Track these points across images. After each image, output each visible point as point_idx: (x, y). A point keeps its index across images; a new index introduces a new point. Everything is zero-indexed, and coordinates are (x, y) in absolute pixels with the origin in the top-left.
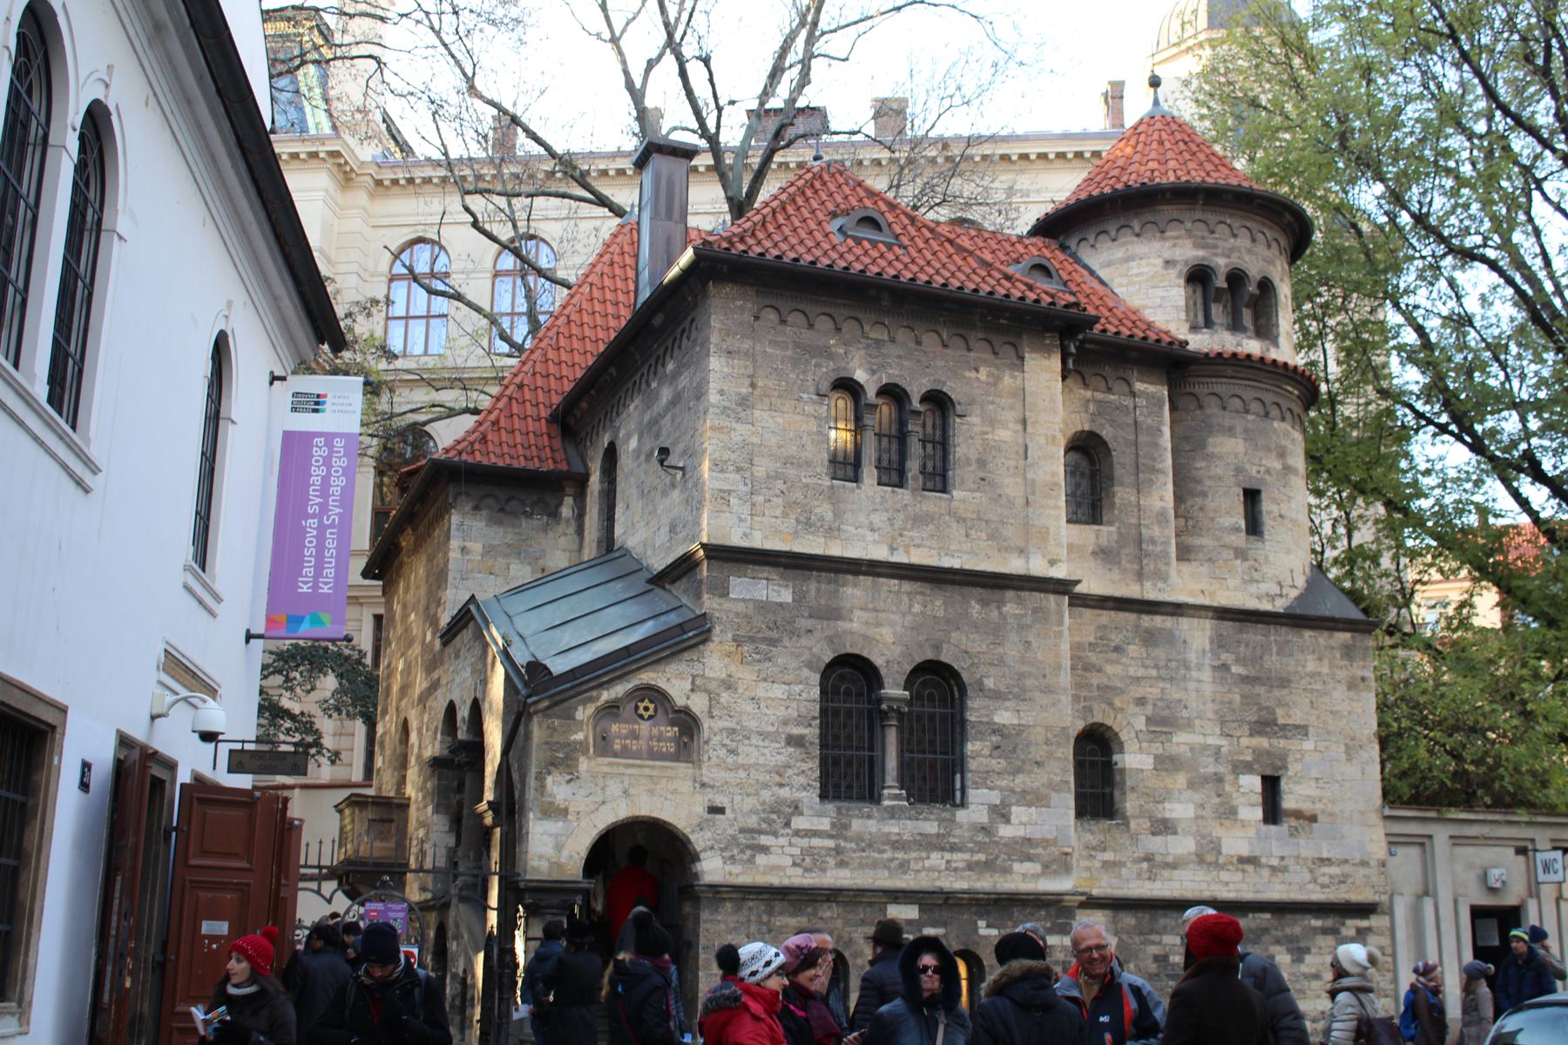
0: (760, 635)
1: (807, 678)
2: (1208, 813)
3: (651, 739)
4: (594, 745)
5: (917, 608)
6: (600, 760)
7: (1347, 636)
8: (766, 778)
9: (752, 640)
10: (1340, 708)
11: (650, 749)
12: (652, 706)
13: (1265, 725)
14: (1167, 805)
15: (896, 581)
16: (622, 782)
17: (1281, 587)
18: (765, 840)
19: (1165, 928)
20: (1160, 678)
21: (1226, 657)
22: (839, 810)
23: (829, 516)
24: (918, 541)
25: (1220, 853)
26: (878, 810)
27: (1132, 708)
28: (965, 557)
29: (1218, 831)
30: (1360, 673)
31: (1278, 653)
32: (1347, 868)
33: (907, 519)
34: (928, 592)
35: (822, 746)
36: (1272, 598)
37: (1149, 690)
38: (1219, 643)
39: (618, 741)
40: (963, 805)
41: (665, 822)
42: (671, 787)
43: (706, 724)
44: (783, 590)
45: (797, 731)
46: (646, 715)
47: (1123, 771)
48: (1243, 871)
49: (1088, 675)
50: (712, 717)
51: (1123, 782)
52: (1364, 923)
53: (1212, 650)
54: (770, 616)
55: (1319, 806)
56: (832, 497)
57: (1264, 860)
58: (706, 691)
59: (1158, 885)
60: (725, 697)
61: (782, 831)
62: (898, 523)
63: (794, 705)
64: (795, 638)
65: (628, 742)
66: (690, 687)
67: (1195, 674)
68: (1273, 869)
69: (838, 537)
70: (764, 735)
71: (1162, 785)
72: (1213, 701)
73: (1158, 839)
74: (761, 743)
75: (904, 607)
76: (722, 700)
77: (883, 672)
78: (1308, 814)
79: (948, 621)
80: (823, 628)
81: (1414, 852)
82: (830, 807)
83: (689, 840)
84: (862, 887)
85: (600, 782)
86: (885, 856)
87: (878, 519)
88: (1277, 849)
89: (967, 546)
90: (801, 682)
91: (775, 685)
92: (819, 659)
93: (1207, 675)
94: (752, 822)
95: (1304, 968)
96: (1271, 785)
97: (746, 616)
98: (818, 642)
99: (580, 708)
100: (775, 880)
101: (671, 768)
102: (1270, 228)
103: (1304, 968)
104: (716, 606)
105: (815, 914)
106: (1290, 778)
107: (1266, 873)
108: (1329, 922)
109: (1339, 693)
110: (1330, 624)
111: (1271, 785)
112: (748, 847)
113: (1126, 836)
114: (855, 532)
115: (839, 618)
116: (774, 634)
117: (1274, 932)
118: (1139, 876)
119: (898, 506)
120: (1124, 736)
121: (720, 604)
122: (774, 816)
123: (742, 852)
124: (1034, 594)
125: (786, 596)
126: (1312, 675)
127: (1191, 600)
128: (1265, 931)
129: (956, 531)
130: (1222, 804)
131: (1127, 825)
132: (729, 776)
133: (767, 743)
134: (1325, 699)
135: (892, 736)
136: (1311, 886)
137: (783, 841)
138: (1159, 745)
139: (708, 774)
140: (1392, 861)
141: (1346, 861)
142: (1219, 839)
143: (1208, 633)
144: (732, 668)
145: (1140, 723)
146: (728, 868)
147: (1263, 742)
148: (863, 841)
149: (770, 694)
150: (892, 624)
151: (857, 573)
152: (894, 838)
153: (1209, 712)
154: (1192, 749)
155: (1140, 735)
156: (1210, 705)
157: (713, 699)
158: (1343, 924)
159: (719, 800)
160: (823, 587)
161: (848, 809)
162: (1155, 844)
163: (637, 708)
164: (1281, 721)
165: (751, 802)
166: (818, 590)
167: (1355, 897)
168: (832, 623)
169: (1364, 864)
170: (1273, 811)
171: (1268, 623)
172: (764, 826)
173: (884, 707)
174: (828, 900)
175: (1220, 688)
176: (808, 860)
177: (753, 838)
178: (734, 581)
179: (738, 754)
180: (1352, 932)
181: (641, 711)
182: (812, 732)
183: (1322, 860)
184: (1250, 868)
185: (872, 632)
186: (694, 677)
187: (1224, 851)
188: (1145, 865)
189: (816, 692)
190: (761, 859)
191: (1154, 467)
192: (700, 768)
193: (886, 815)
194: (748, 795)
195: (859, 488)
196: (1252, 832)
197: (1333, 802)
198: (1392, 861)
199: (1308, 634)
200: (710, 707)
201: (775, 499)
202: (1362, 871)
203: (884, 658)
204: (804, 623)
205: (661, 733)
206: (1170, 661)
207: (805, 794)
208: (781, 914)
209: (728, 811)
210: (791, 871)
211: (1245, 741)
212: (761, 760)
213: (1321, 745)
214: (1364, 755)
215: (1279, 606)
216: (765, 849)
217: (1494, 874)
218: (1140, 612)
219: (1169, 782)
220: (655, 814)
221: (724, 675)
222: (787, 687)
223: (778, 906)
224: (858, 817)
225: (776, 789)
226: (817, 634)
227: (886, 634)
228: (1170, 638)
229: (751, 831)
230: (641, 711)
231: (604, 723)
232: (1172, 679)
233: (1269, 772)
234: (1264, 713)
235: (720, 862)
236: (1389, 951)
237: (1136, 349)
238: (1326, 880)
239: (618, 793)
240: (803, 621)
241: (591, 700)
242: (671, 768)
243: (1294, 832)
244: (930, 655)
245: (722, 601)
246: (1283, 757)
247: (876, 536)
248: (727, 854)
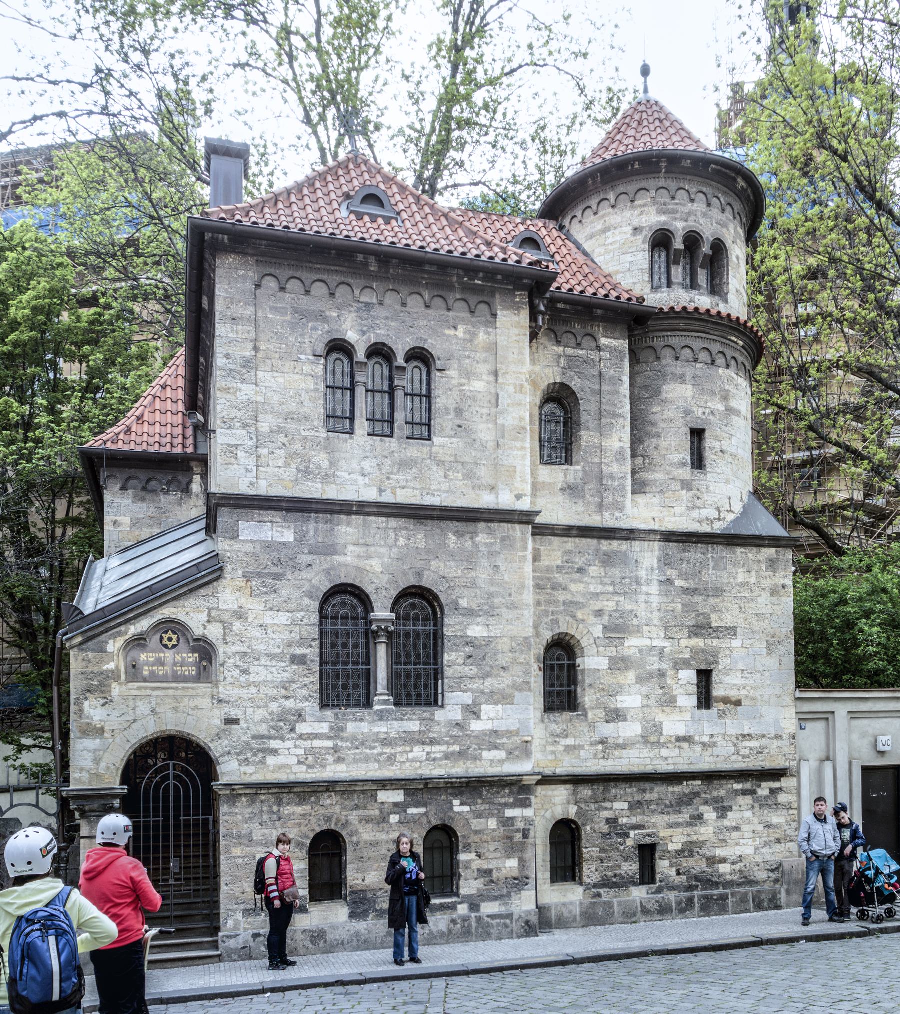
0: (266, 571)
1: (308, 606)
2: (652, 702)
5: (402, 541)
7: (773, 550)
8: (273, 692)
9: (260, 575)
10: (764, 611)
13: (701, 628)
14: (619, 698)
15: (384, 519)
17: (720, 512)
18: (274, 744)
19: (616, 796)
20: (615, 593)
21: (671, 573)
22: (336, 715)
23: (325, 464)
24: (403, 483)
25: (661, 734)
26: (369, 714)
27: (592, 619)
28: (444, 495)
29: (660, 717)
30: (782, 581)
31: (714, 569)
32: (764, 742)
33: (394, 464)
34: (411, 527)
35: (322, 663)
36: (711, 521)
37: (606, 603)
38: (666, 562)
40: (442, 706)
43: (221, 650)
44: (285, 531)
45: (299, 651)
47: (583, 671)
48: (680, 748)
49: (555, 593)
51: (584, 680)
52: (776, 785)
53: (659, 568)
54: (275, 554)
55: (743, 692)
56: (328, 447)
57: (697, 738)
58: (221, 621)
59: (610, 762)
60: (237, 626)
61: (288, 736)
62: (386, 469)
63: (297, 629)
67: (644, 588)
68: (704, 745)
69: (334, 482)
70: (271, 656)
71: (615, 681)
72: (659, 610)
73: (611, 726)
74: (269, 663)
75: (391, 541)
77: (373, 597)
78: (734, 699)
79: (428, 551)
80: (321, 563)
81: (820, 726)
82: (329, 713)
84: (356, 778)
85: (131, 703)
86: (375, 751)
87: (368, 465)
88: (708, 731)
89: (445, 486)
90: (302, 610)
92: (318, 589)
93: (654, 589)
94: (263, 729)
95: (726, 823)
96: (705, 677)
97: (254, 555)
98: (317, 574)
100: (283, 777)
102: (725, 193)
103: (726, 823)
104: (227, 548)
105: (317, 802)
106: (720, 671)
107: (698, 748)
108: (748, 786)
109: (764, 598)
110: (757, 541)
111: (705, 677)
112: (259, 750)
113: (584, 724)
114: (348, 477)
115: (335, 552)
116: (278, 570)
117: (703, 795)
118: (595, 755)
119: (386, 453)
120: (584, 643)
121: (231, 546)
122: (282, 724)
123: (255, 755)
124: (502, 524)
125: (289, 536)
126: (742, 585)
127: (643, 526)
128: (697, 794)
129: (437, 473)
130: (664, 695)
131: (586, 715)
132: (243, 693)
133: (274, 663)
134: (752, 605)
135: (382, 651)
136: (734, 758)
137: (289, 744)
138: (614, 649)
139: (224, 691)
140: (801, 735)
141: (764, 736)
142: (661, 723)
143: (657, 553)
144: (243, 601)
145: (598, 631)
146: (244, 769)
147: (699, 642)
148: (357, 740)
149: (276, 622)
150: (380, 556)
151: (350, 513)
152: (383, 736)
153: (656, 618)
154: (641, 651)
155: (598, 641)
156: (656, 614)
157: (227, 628)
158: (760, 786)
159: (234, 713)
160: (321, 526)
161: (344, 715)
162: (607, 730)
164: (714, 624)
165: (261, 713)
166: (317, 530)
167: (769, 764)
168: (329, 558)
169: (778, 737)
170: (705, 699)
171: (707, 543)
172: (273, 732)
173: (374, 627)
174: (328, 791)
175: (665, 599)
176: (311, 758)
177: (264, 743)
178: (242, 524)
179: (249, 674)
180: (766, 792)
182: (312, 652)
183: (744, 736)
184: (685, 745)
185: (363, 563)
186: (210, 610)
187: (665, 733)
188: (600, 747)
189: (315, 618)
190: (271, 760)
191: (614, 412)
193: (376, 718)
194: (259, 707)
195: (351, 438)
196: (688, 716)
197: (755, 688)
198: (801, 735)
199: (739, 550)
200: (225, 635)
201: (278, 451)
202: (776, 743)
203: (374, 586)
204: (304, 559)
206: (624, 578)
207: (307, 704)
208: (289, 804)
209: (242, 722)
210: (296, 769)
211: (684, 642)
212: (270, 678)
213: (747, 643)
214: (782, 649)
215: (718, 527)
216: (274, 752)
217: (882, 739)
218: (600, 538)
219: (621, 679)
221: (236, 607)
222: (290, 615)
223: (286, 798)
224: (352, 720)
226: (316, 568)
227: (376, 565)
228: (623, 559)
229: (262, 737)
232: (625, 593)
233: (703, 667)
234: (701, 618)
236: (795, 805)
237: (600, 306)
238: (747, 752)
240: (304, 557)
243: (722, 715)
244: (413, 581)
245: (233, 542)
246: (715, 655)
247: (367, 480)
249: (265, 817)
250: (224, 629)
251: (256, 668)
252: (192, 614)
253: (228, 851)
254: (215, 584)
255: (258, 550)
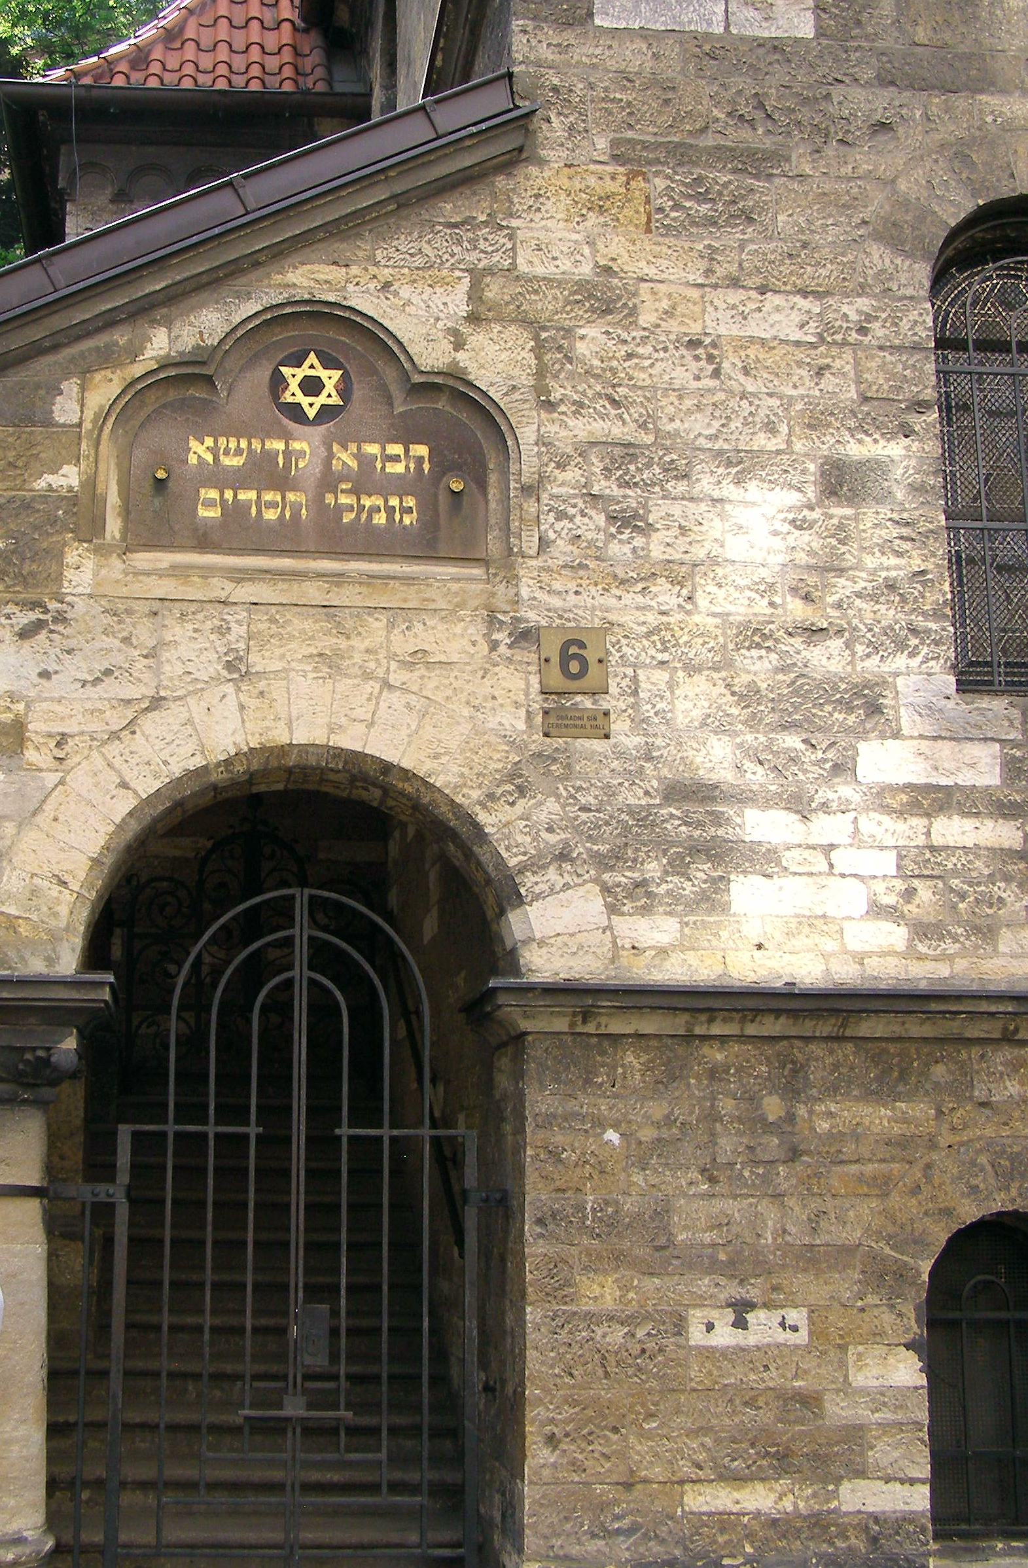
0: (709, 141)
3: (329, 481)
4: (126, 512)
6: (143, 559)
9: (681, 154)
11: (328, 518)
12: (331, 378)
16: (222, 630)
39: (213, 494)
41: (387, 768)
42: (402, 644)
46: (311, 406)
50: (550, 406)
54: (739, 82)
61: (824, 794)
63: (844, 362)
64: (830, 151)
65: (250, 495)
66: (463, 310)
76: (581, 348)
83: (477, 828)
90: (862, 290)
91: (778, 300)
98: (915, 160)
99: (71, 386)
101: (408, 580)
116: (759, 138)
121: (563, 49)
122: (792, 741)
123: (678, 867)
144: (615, 247)
149: (754, 329)
163: (278, 383)
172: (757, 776)
179: (647, 530)
181: (294, 394)
186: (477, 277)
192: (512, 579)
194: (692, 669)
200: (541, 372)
205: (365, 462)
209: (619, 726)
220: (349, 741)
225: (797, 642)
230: (294, 394)
231: (160, 436)
235: (597, 904)
239: (209, 666)
240: (858, 95)
241: (108, 359)
242: (408, 580)
245: (569, 36)
248: (620, 877)
249: (728, 1145)
250: (539, 349)
251: (676, 509)
252: (405, 292)
253: (562, 1290)
254: (500, 181)
255: (672, 65)
